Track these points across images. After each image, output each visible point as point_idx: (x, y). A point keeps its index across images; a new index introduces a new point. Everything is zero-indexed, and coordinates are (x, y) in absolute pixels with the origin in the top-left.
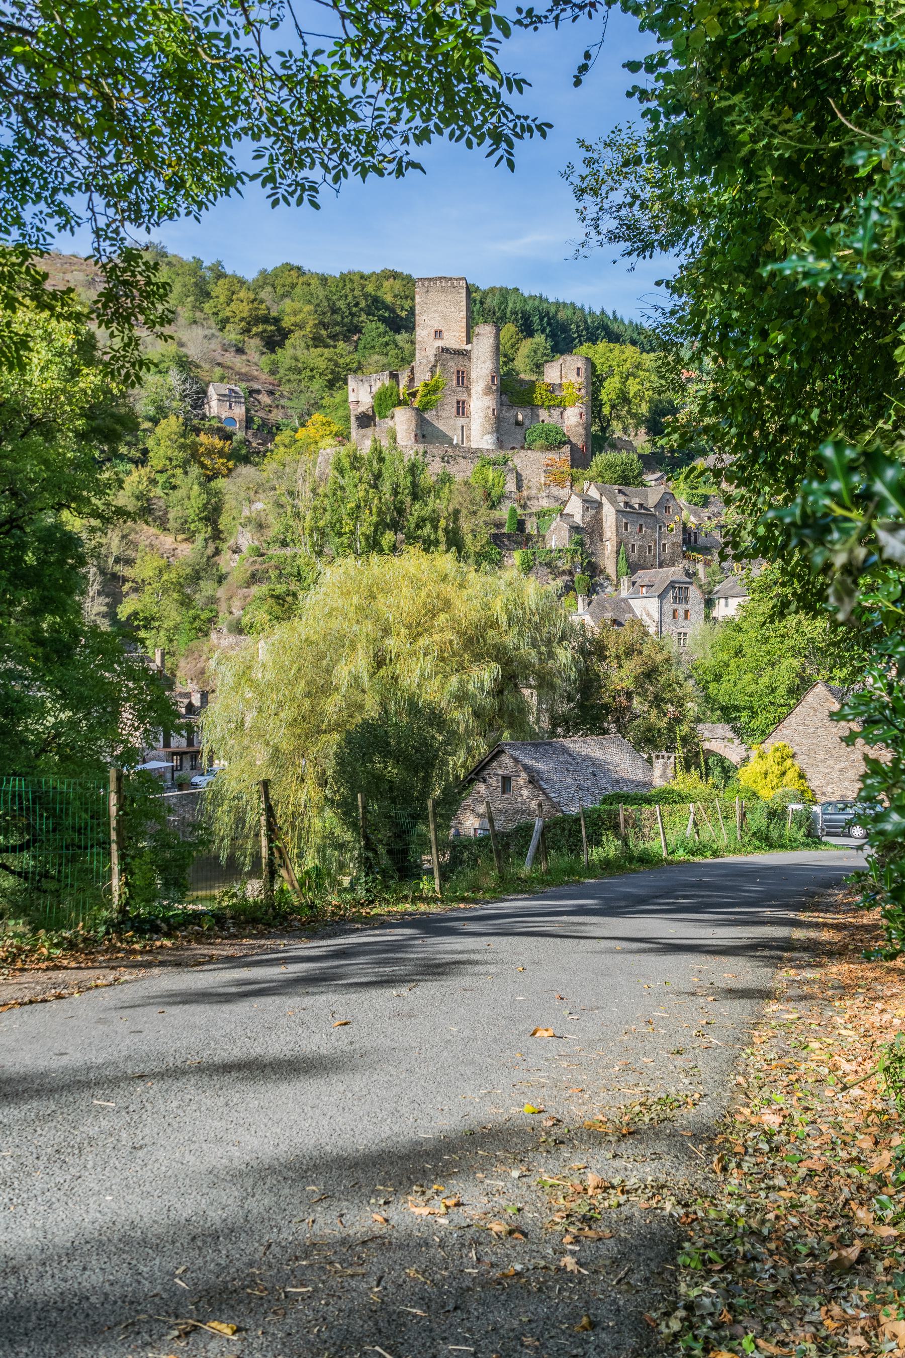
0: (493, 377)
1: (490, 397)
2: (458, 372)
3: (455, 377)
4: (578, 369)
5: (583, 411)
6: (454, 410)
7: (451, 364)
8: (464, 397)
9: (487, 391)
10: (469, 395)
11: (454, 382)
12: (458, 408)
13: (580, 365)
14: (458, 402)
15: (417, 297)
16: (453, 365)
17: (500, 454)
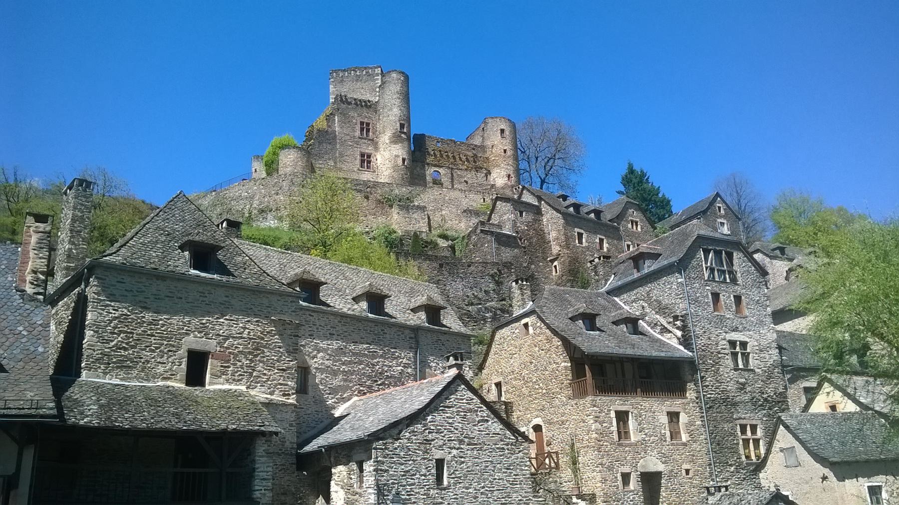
0: (402, 126)
1: (398, 146)
2: (362, 123)
3: (358, 127)
4: (502, 131)
5: (511, 173)
6: (358, 162)
7: (352, 114)
8: (369, 150)
9: (396, 139)
10: (376, 149)
11: (358, 133)
12: (362, 161)
13: (503, 127)
14: (362, 155)
15: (331, 86)
16: (356, 117)
17: (404, 191)
